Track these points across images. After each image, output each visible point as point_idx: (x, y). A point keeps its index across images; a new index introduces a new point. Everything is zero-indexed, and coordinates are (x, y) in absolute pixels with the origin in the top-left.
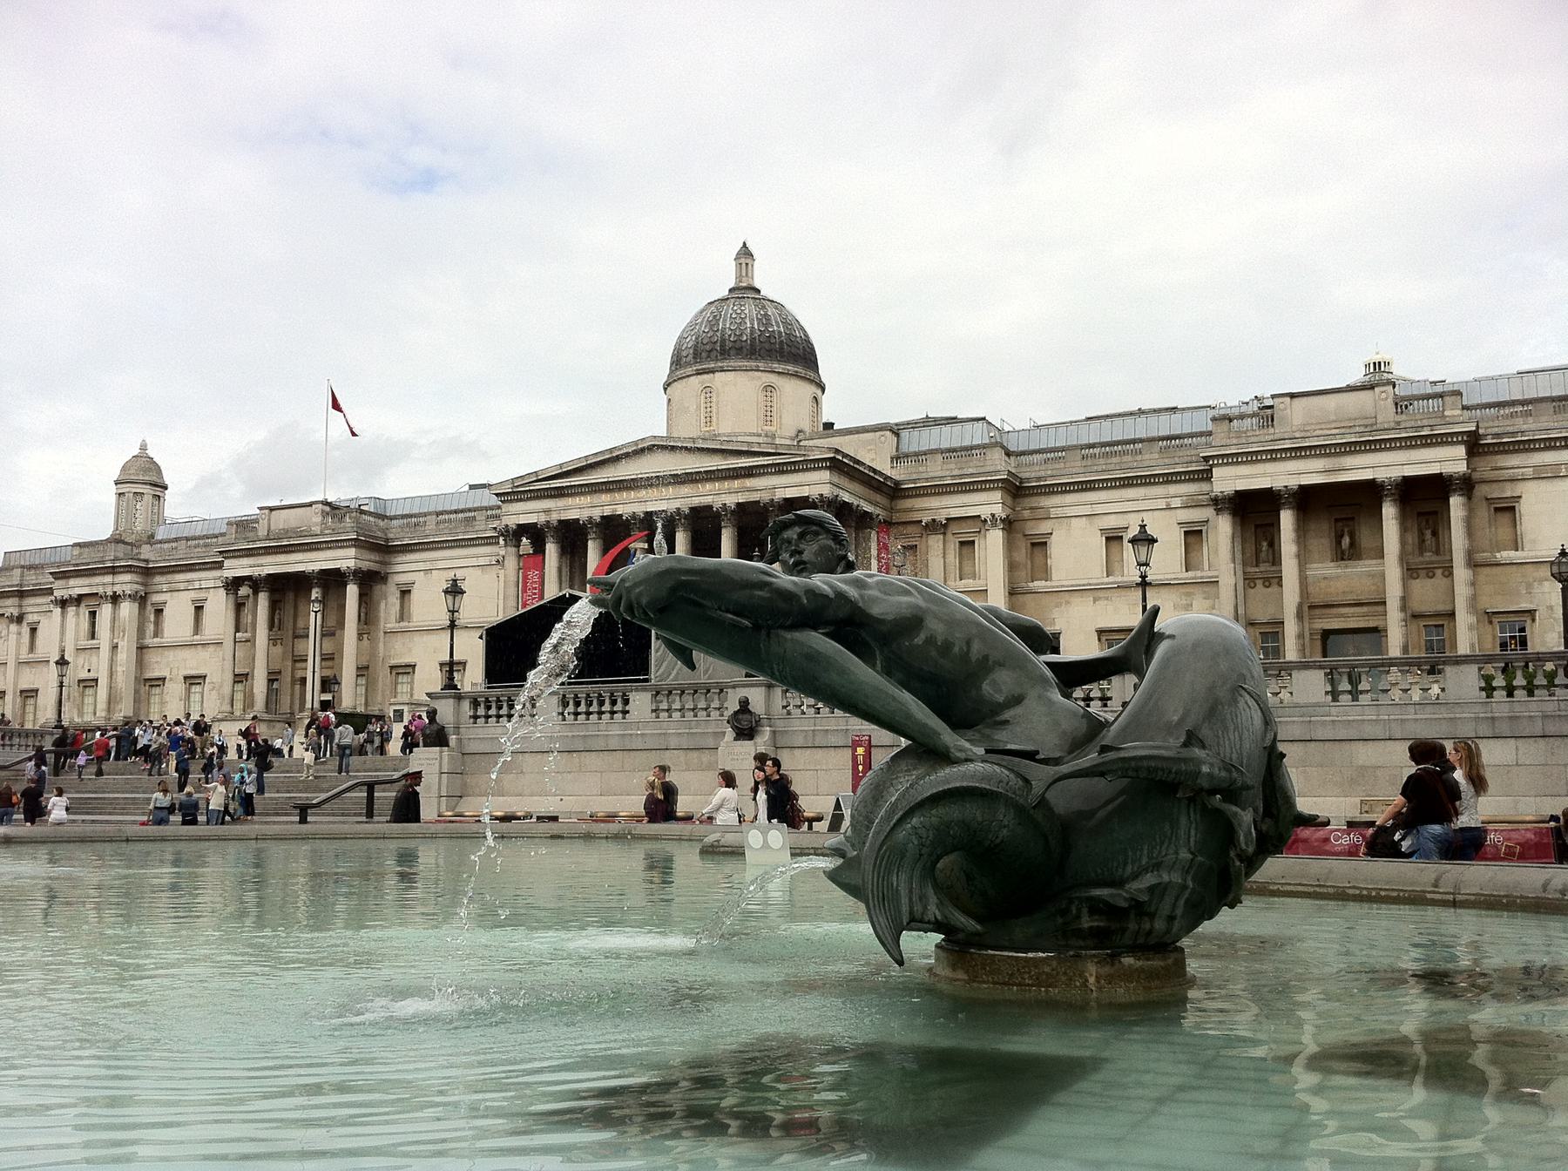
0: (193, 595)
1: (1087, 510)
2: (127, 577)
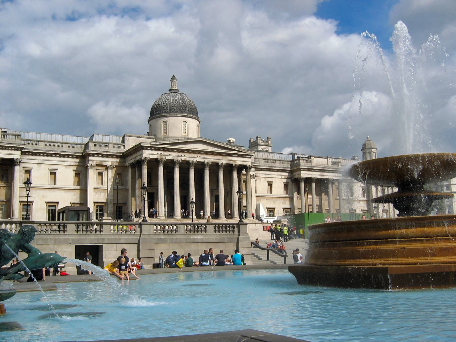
1: (264, 176)
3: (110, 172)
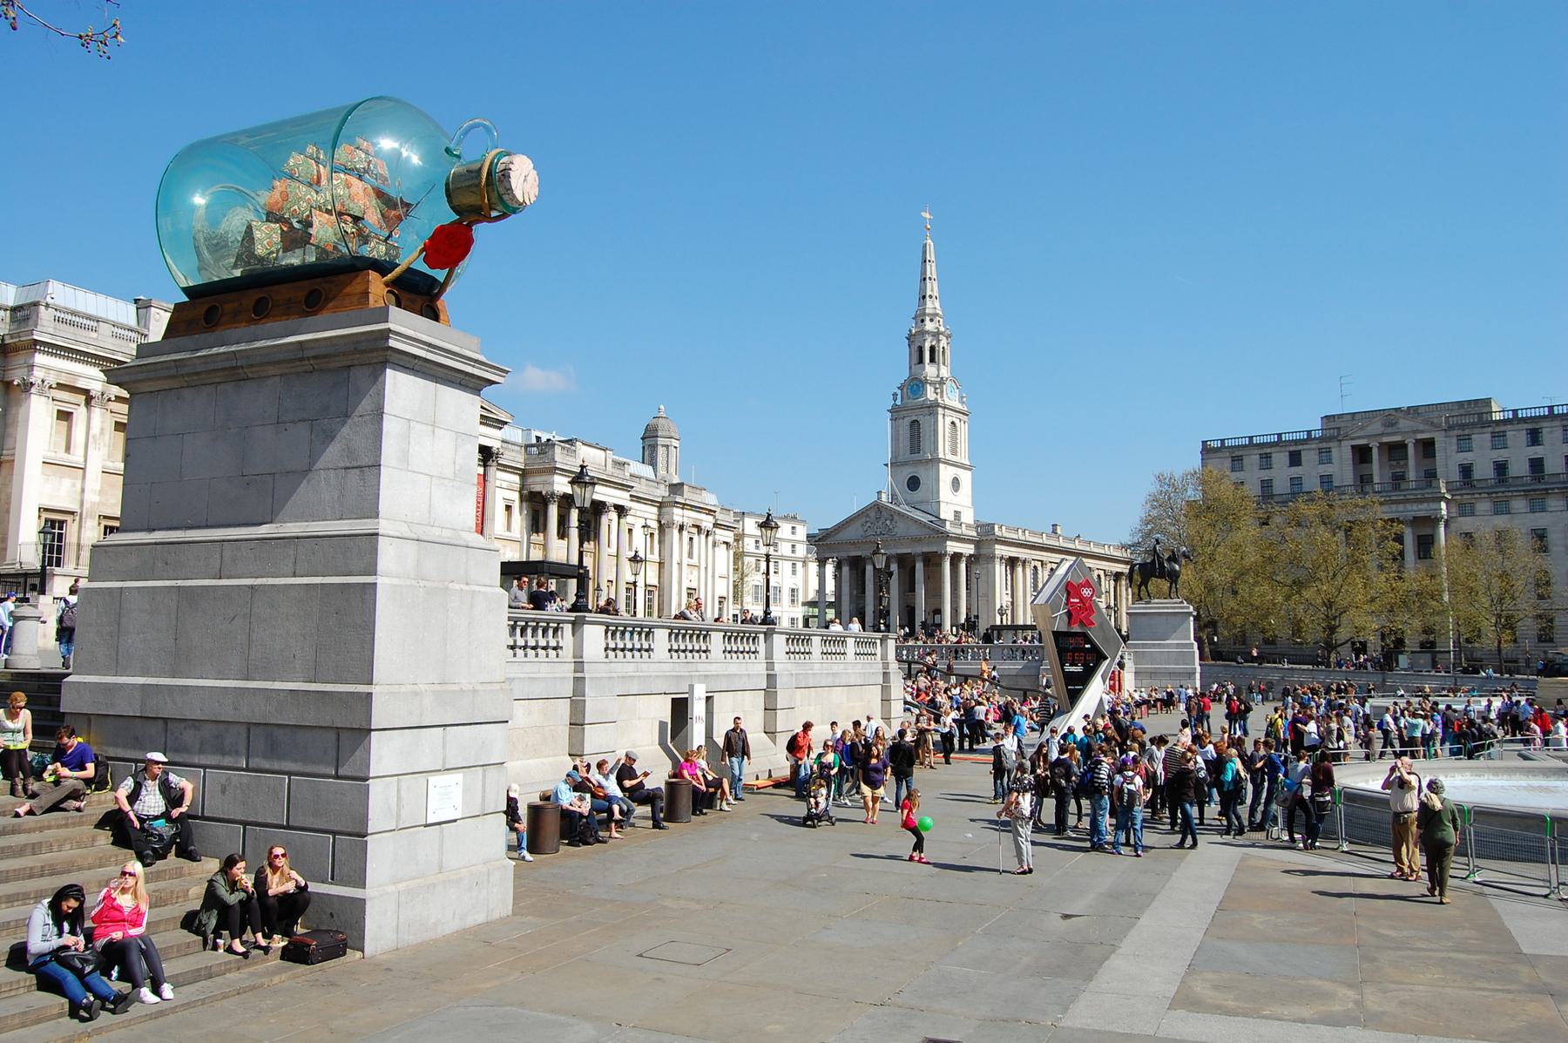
3: (97, 412)
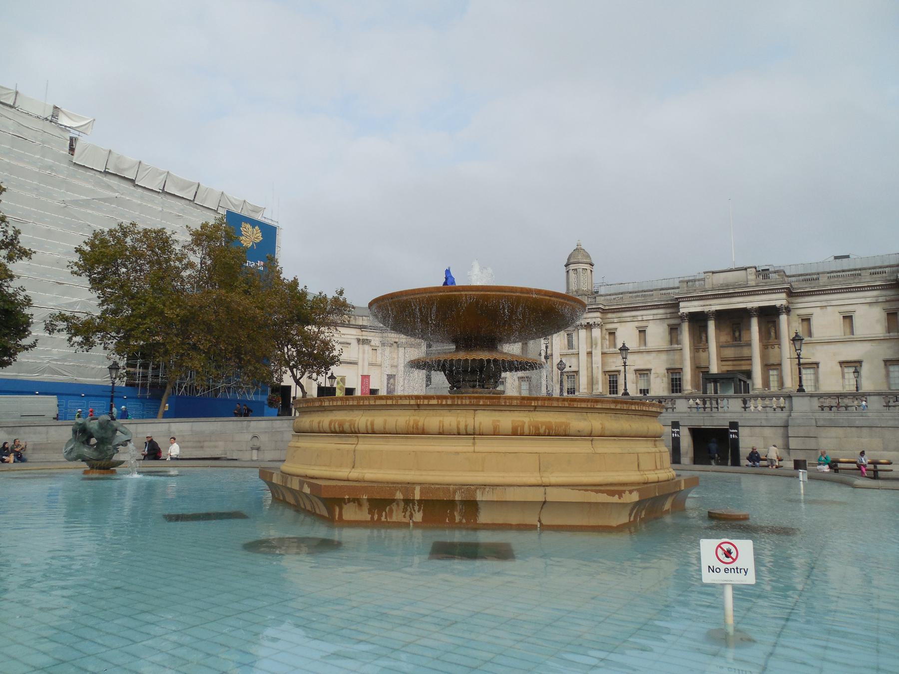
0: (637, 324)
2: (598, 314)
